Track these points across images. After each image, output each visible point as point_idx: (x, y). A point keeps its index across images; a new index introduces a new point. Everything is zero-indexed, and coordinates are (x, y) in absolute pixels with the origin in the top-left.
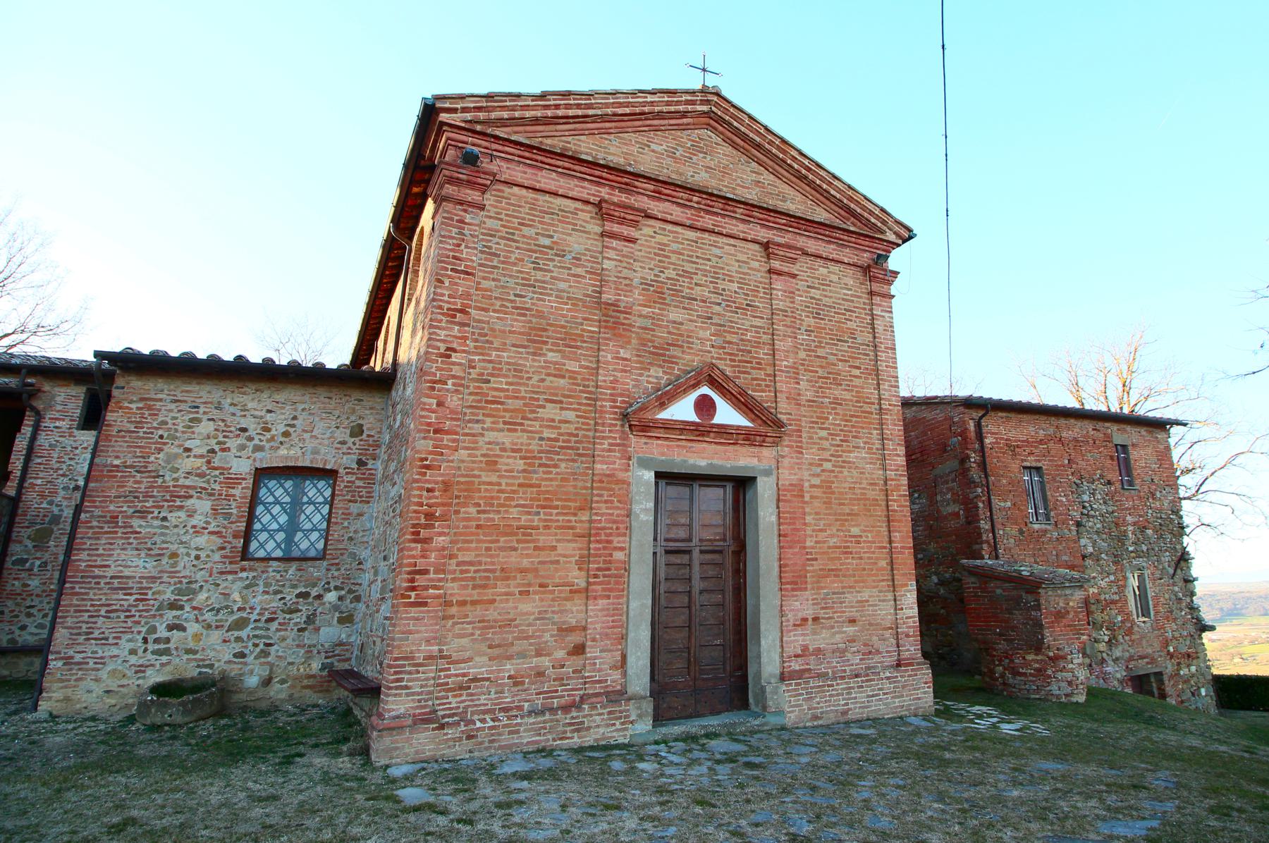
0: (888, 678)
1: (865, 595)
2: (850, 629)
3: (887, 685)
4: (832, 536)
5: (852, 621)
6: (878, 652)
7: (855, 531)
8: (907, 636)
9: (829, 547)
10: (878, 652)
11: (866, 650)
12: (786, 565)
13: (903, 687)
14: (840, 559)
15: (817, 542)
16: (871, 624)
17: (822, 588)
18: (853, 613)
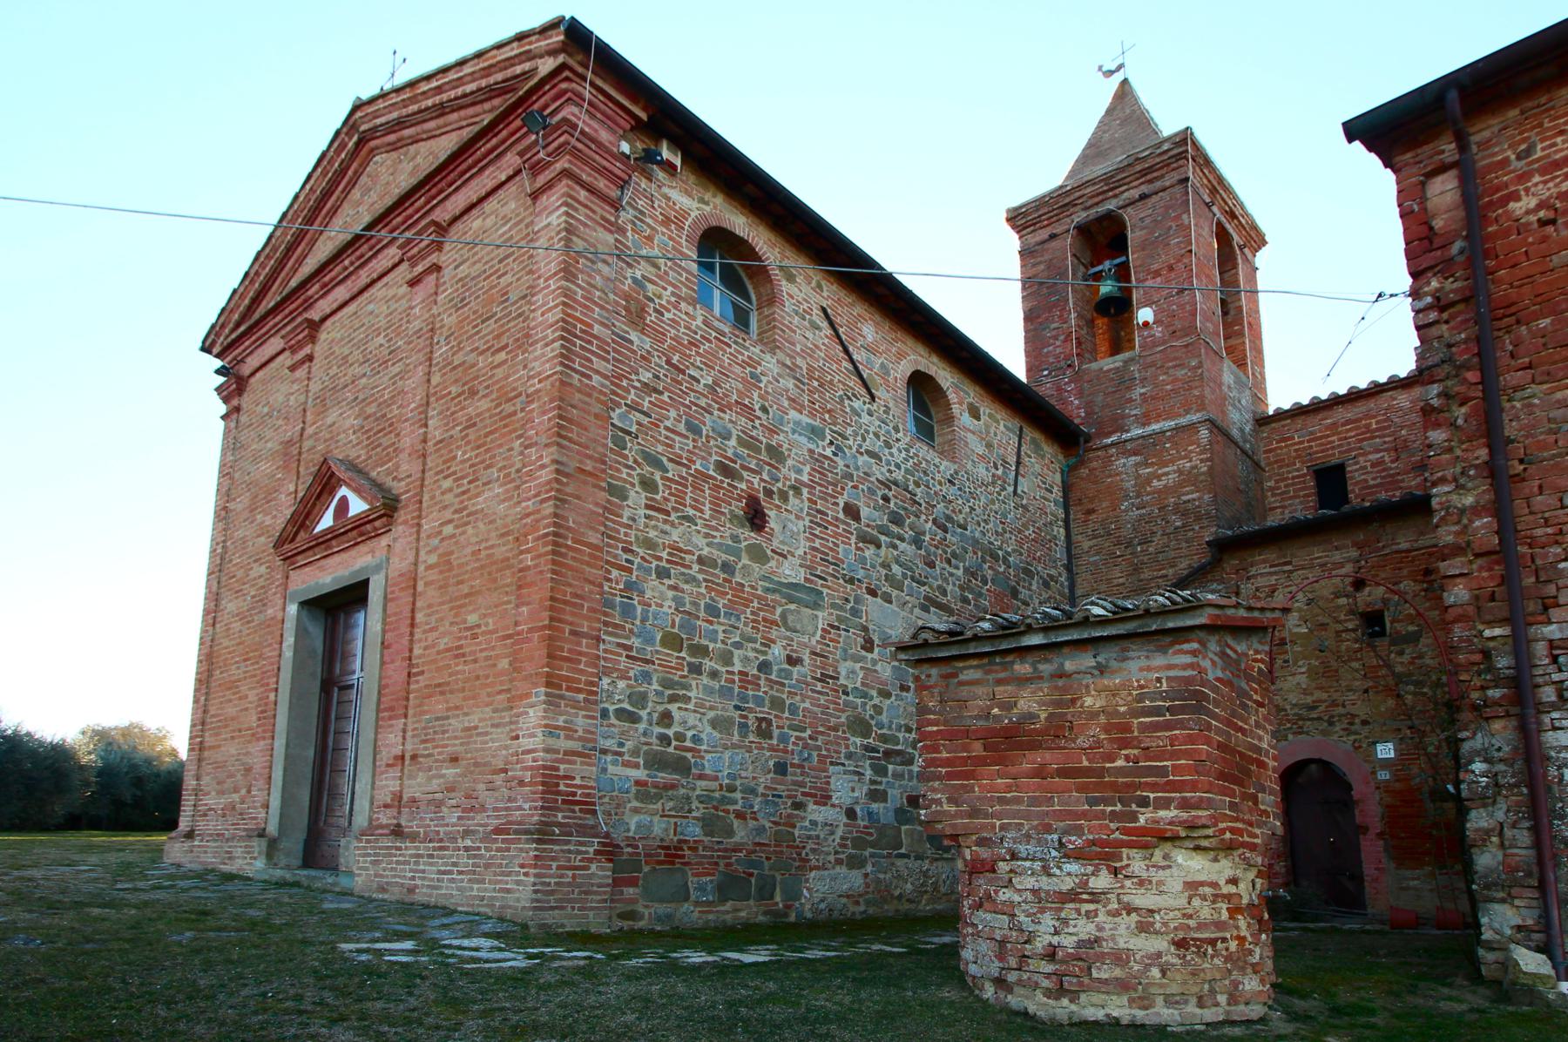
0: (467, 849)
1: (474, 719)
2: (450, 772)
3: (465, 861)
4: (444, 634)
5: (454, 760)
6: (483, 809)
7: (472, 619)
8: (521, 783)
9: (438, 653)
10: (483, 809)
11: (467, 803)
12: (387, 686)
13: (487, 866)
14: (449, 666)
15: (426, 648)
16: (476, 764)
17: (425, 712)
18: (456, 747)
